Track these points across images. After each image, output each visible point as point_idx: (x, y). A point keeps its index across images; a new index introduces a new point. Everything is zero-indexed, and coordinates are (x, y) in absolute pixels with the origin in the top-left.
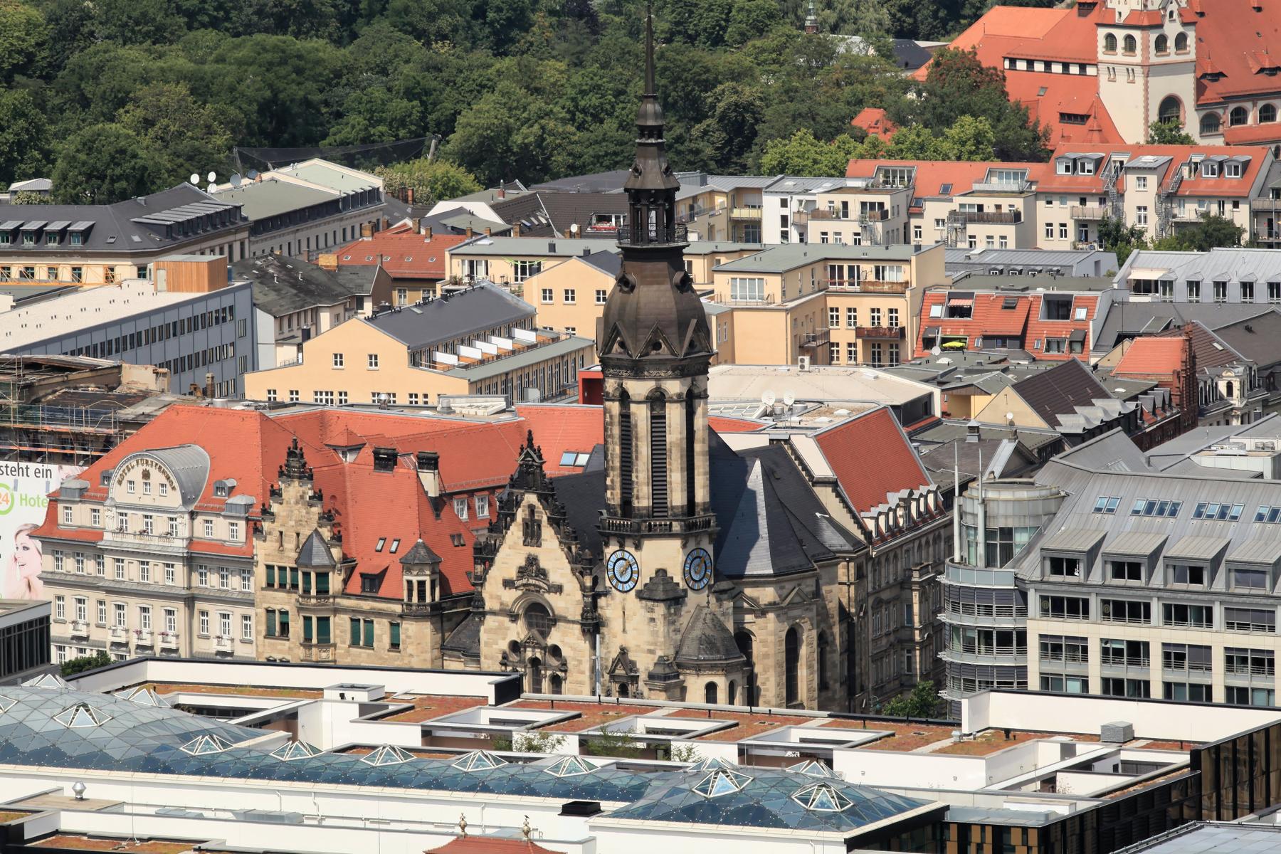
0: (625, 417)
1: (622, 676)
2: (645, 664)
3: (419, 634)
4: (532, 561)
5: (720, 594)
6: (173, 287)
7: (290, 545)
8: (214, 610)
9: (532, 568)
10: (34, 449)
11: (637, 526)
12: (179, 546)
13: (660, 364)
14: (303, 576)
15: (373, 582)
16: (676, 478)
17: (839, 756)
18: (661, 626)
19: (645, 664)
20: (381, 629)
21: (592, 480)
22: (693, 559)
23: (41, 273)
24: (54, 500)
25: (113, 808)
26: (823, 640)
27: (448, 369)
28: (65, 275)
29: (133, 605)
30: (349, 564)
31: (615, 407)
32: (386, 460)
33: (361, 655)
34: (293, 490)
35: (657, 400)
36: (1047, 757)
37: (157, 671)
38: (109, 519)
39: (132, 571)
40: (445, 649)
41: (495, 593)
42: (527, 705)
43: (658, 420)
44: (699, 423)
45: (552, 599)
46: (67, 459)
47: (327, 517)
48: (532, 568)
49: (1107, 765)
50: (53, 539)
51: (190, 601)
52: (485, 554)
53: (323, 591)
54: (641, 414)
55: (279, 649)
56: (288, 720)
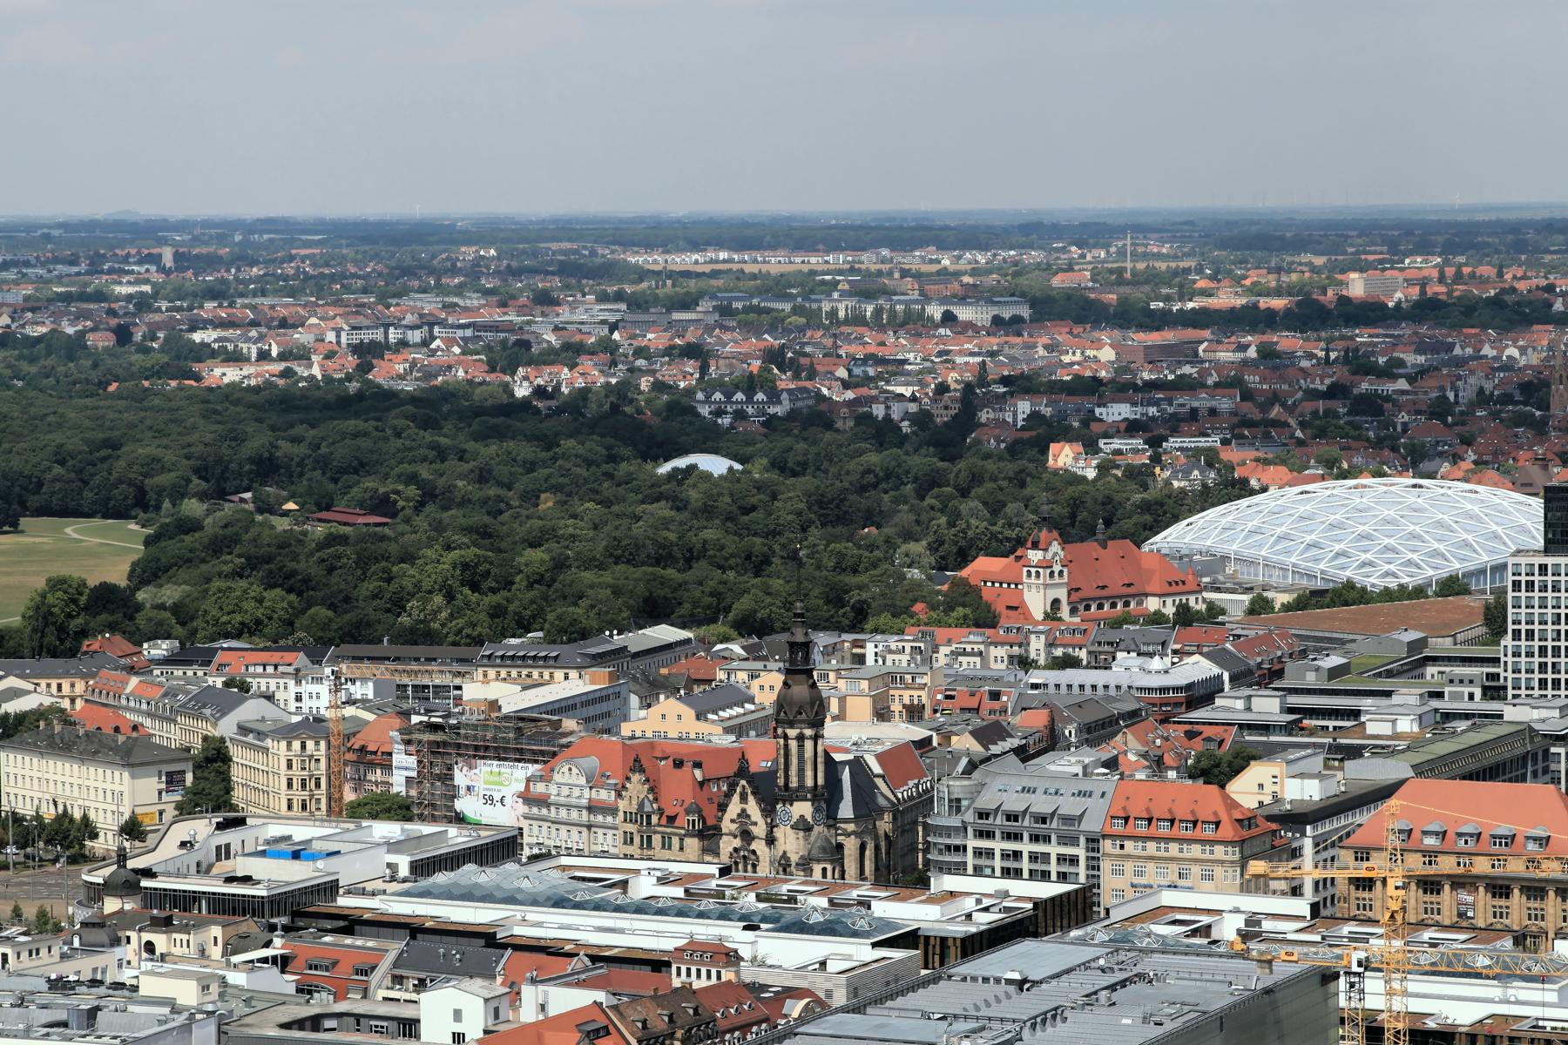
0: (786, 746)
1: (784, 865)
2: (794, 858)
3: (693, 844)
4: (744, 811)
5: (829, 827)
6: (593, 683)
7: (634, 802)
8: (600, 831)
9: (743, 814)
10: (521, 756)
11: (791, 796)
12: (584, 802)
13: (802, 722)
14: (639, 816)
15: (672, 820)
16: (809, 773)
17: (874, 904)
18: (801, 841)
19: (794, 858)
20: (675, 841)
21: (771, 774)
22: (817, 810)
23: (535, 674)
24: (528, 780)
25: (539, 925)
26: (877, 848)
27: (713, 721)
28: (546, 677)
29: (563, 829)
30: (661, 812)
31: (782, 741)
32: (679, 764)
33: (666, 854)
34: (636, 777)
35: (801, 738)
36: (969, 904)
37: (565, 861)
38: (553, 790)
39: (563, 813)
40: (705, 851)
41: (727, 825)
42: (733, 878)
43: (801, 746)
44: (820, 749)
45: (752, 828)
46: (536, 762)
47: (651, 790)
48: (743, 814)
49: (996, 909)
50: (528, 798)
51: (589, 827)
52: (722, 808)
53: (649, 823)
54: (793, 744)
55: (629, 850)
56: (624, 884)
